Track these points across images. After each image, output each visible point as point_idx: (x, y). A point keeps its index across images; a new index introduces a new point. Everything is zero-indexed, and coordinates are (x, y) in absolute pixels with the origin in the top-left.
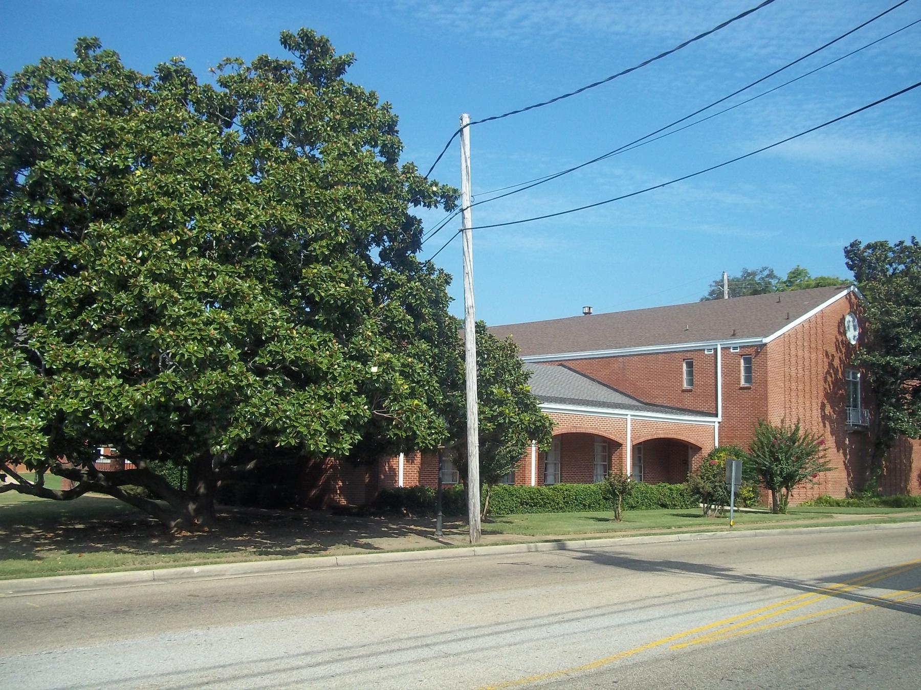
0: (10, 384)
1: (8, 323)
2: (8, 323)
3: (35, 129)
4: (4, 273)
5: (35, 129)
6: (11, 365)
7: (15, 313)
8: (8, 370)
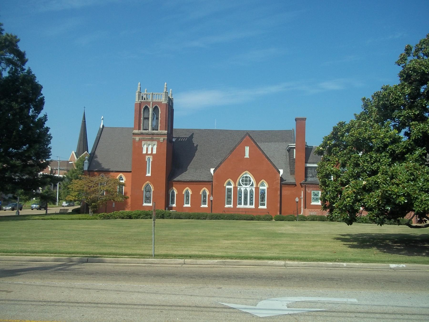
0: (424, 181)
1: (421, 154)
2: (421, 154)
3: (426, 68)
4: (418, 133)
5: (426, 68)
6: (424, 173)
7: (424, 149)
8: (423, 175)
